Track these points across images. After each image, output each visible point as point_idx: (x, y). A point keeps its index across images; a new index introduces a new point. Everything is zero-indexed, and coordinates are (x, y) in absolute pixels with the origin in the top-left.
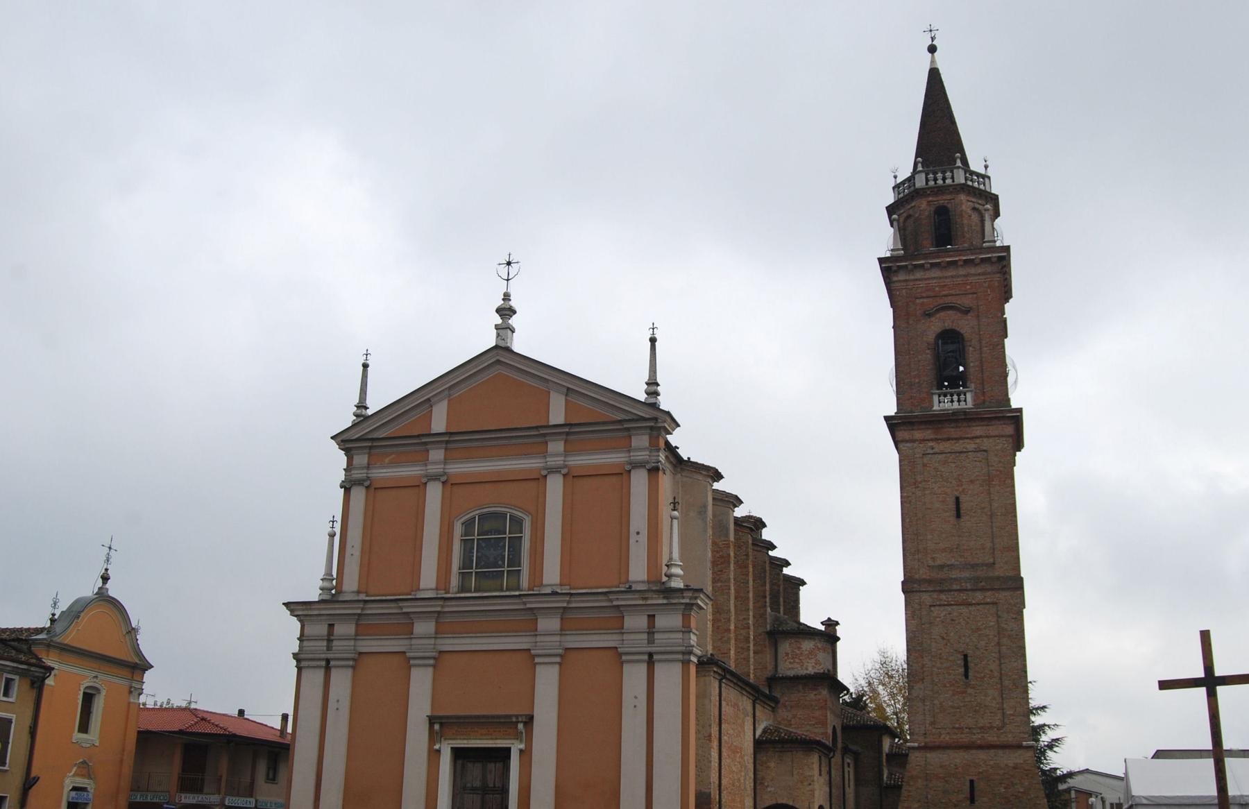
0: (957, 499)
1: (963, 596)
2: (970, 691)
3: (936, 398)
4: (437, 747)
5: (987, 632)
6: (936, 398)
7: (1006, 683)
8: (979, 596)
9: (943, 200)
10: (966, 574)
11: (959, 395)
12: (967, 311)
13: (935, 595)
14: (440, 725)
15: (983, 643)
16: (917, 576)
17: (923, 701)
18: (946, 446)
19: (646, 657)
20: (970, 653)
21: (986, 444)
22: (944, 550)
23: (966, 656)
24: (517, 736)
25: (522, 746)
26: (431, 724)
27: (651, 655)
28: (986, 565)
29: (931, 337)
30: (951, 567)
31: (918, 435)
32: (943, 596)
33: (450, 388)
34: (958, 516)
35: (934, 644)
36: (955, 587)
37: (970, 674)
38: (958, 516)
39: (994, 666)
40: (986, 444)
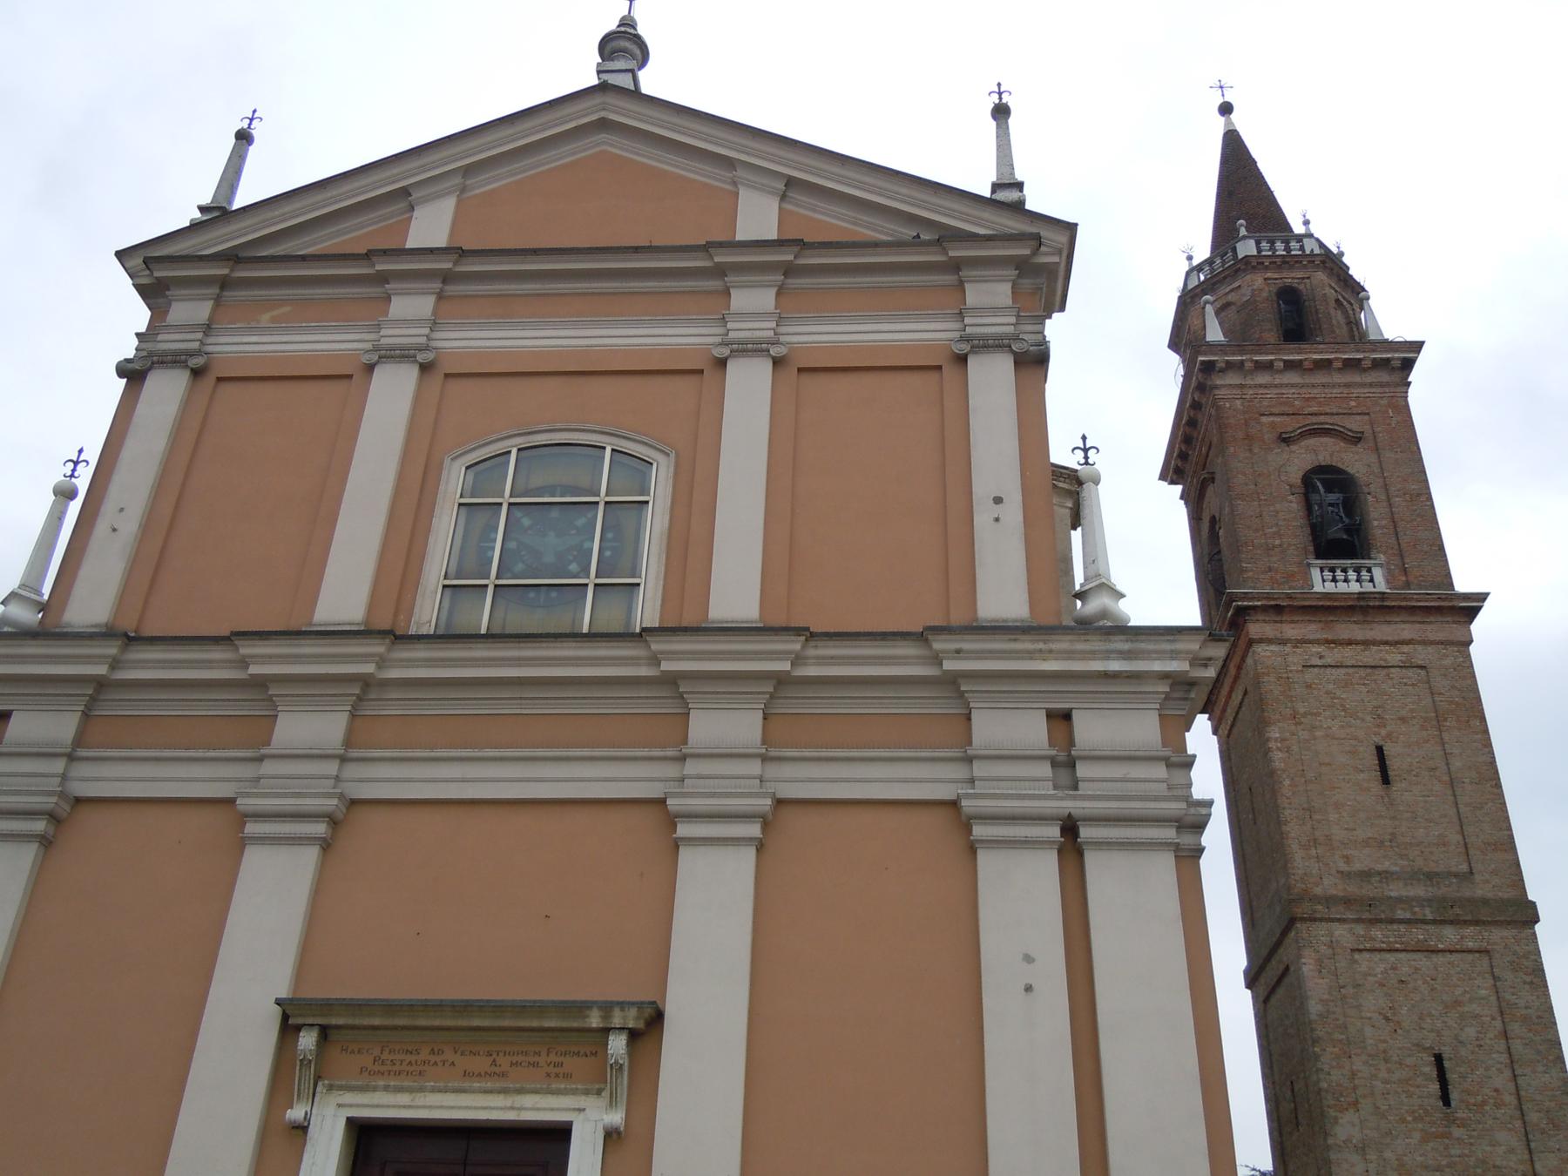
0: (1380, 750)
1: (1418, 934)
2: (1457, 1132)
3: (1316, 574)
4: (296, 1113)
5: (1474, 1008)
6: (1316, 574)
7: (1533, 1117)
8: (1450, 935)
9: (1291, 277)
10: (1419, 891)
11: (1357, 570)
12: (1356, 439)
13: (1360, 929)
14: (320, 1030)
15: (1471, 1032)
16: (1318, 891)
17: (1362, 1149)
18: (1348, 655)
19: (1054, 832)
20: (1447, 1052)
21: (1422, 654)
22: (1366, 843)
23: (1439, 1059)
24: (598, 1082)
25: (616, 1118)
26: (288, 1029)
27: (1070, 828)
28: (1456, 875)
29: (1295, 474)
30: (1386, 876)
31: (1291, 631)
32: (1377, 933)
33: (468, 171)
34: (1386, 780)
35: (1368, 1031)
36: (1400, 914)
37: (1454, 1096)
38: (1386, 780)
39: (1501, 1080)
40: (1422, 654)
